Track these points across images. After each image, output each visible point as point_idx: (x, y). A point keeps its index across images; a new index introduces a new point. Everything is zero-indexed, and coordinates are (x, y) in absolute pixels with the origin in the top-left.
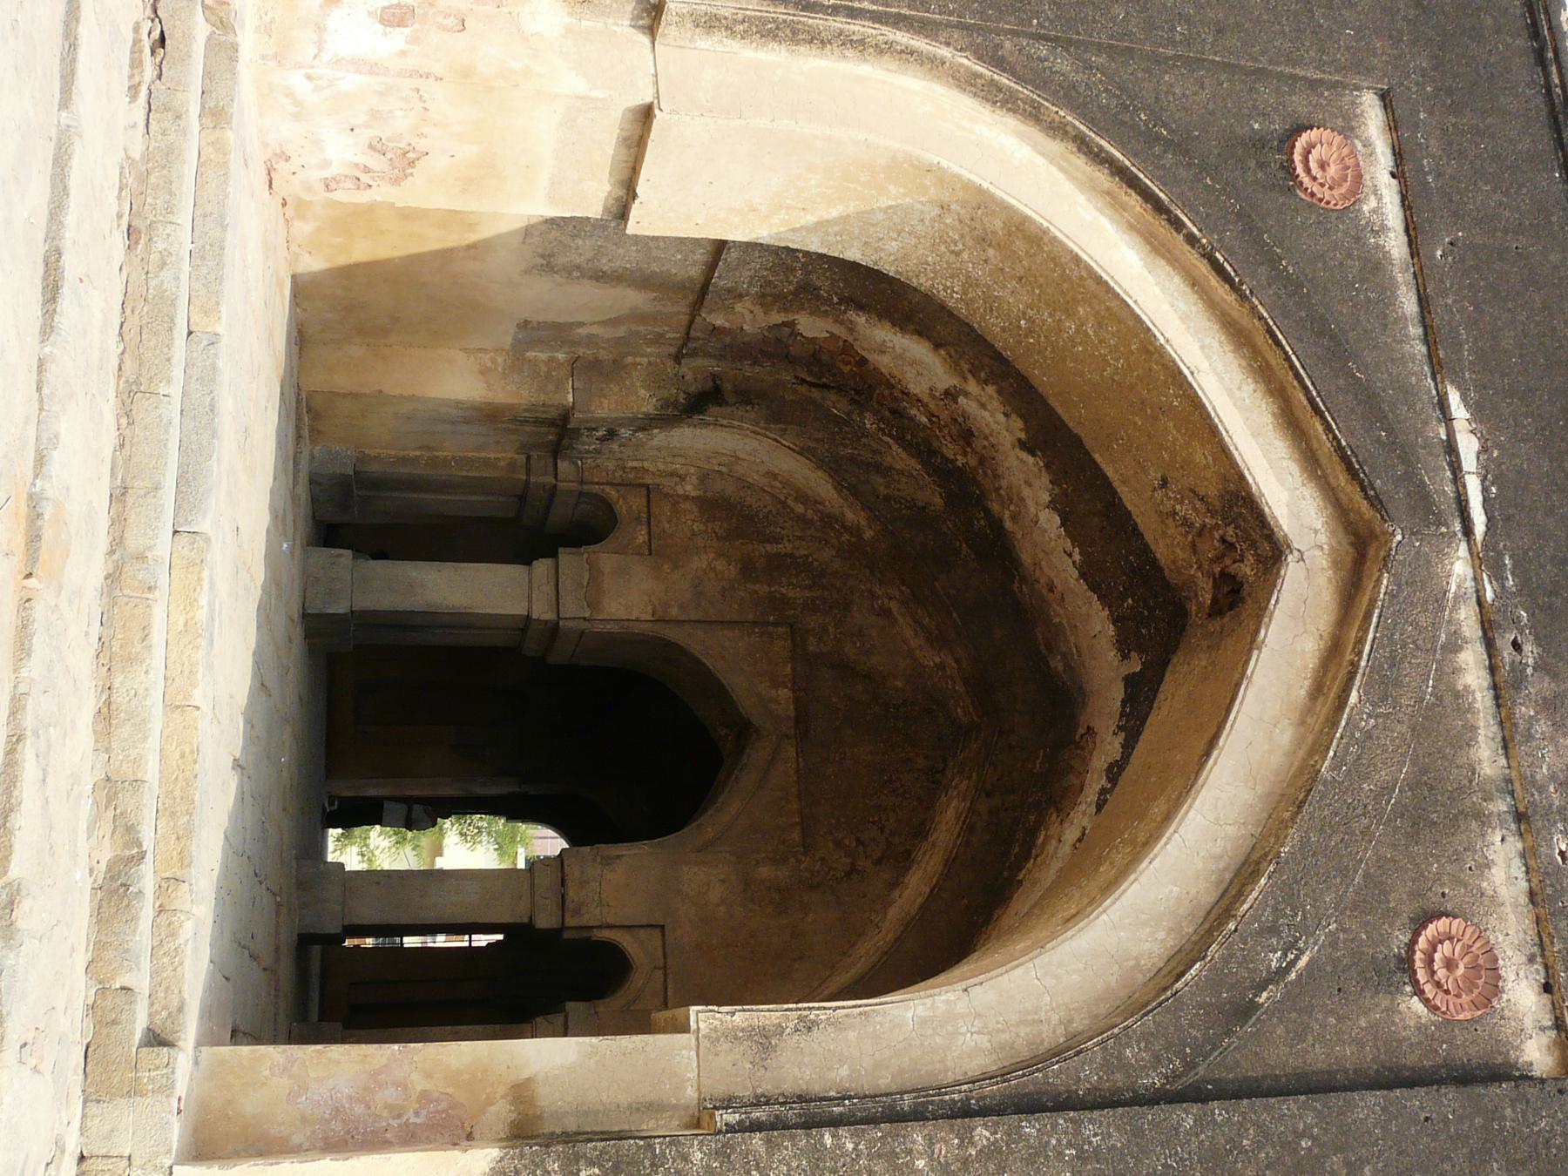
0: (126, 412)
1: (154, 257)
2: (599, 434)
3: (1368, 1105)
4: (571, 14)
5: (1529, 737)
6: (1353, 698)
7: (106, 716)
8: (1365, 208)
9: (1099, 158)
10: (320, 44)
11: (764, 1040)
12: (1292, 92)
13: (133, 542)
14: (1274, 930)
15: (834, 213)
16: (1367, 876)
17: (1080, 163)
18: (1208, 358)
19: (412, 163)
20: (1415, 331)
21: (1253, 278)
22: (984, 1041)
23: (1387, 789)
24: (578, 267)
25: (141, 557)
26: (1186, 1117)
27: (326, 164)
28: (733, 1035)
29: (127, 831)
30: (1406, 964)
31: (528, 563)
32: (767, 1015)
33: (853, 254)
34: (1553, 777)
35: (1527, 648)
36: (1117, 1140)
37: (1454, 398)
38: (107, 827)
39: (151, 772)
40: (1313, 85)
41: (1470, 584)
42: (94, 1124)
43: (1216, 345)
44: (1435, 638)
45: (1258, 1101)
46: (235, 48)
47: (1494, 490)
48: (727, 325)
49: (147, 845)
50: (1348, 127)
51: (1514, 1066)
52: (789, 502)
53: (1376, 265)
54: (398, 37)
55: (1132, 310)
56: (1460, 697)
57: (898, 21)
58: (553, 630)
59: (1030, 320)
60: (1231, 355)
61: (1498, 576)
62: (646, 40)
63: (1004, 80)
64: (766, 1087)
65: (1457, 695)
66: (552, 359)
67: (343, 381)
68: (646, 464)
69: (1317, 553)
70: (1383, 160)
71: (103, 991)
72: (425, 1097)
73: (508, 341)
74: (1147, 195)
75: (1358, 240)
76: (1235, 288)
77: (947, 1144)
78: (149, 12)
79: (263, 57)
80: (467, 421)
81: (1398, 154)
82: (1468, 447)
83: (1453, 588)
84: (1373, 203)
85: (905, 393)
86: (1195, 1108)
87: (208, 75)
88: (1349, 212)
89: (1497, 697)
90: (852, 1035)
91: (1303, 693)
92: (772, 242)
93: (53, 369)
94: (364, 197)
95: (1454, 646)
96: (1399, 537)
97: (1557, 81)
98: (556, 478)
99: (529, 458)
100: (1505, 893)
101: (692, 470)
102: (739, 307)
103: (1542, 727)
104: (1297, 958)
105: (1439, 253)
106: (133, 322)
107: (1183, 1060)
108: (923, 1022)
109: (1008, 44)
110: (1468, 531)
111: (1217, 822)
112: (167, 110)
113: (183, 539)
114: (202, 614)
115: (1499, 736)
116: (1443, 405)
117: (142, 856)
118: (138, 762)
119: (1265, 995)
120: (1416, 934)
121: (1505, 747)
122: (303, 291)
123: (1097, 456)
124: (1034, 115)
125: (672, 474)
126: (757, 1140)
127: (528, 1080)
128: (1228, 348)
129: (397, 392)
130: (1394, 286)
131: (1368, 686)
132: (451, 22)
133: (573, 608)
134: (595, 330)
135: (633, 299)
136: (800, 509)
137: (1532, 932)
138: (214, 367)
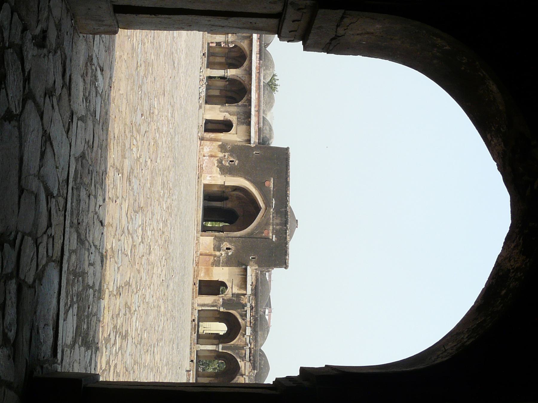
26: (248, 239)
29: (198, 222)
37: (274, 199)
50: (270, 181)
53: (270, 190)
56: (270, 218)
82: (274, 202)
88: (269, 187)
95: (270, 215)
103: (275, 220)
133: (225, 206)
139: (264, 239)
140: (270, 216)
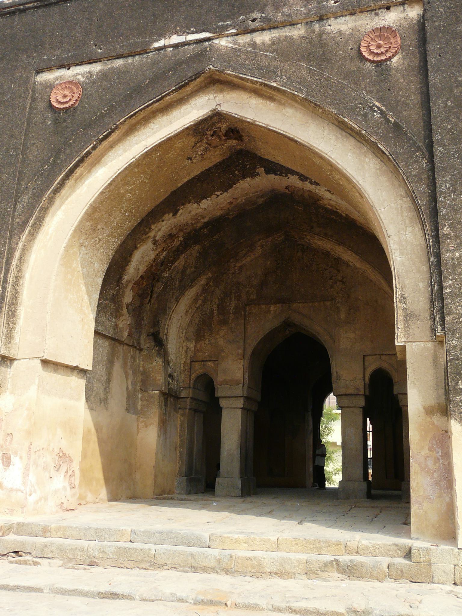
0: (162, 566)
1: (101, 555)
2: (170, 381)
3: (434, 79)
4: (6, 392)
5: (289, 15)
6: (274, 84)
7: (281, 574)
8: (82, 80)
9: (62, 184)
10: (18, 490)
11: (409, 316)
12: (36, 108)
13: (213, 564)
14: (365, 116)
15: (84, 288)
16: (344, 79)
17: (64, 192)
18: (140, 141)
19: (64, 454)
20: (130, 60)
21: (109, 124)
22: (409, 229)
23: (310, 71)
24: (105, 389)
25: (219, 561)
26: (439, 150)
27: (64, 488)
28: (407, 328)
29: (326, 566)
30: (379, 64)
31: (221, 409)
32: (399, 315)
33: (100, 281)
34: (305, 6)
35: (255, 16)
36: (448, 177)
37: (156, 45)
38: (325, 574)
39: (303, 557)
40: (33, 100)
41: (229, 39)
42: (441, 579)
43: (135, 138)
44: (251, 52)
45: (433, 122)
46: (19, 524)
47: (192, 29)
48: (128, 330)
49: (332, 558)
50: (50, 86)
51: (419, 21)
52: (197, 306)
53: (104, 76)
54: (15, 460)
55: (122, 171)
56: (275, 43)
57: (8, 263)
58: (247, 399)
59: (126, 211)
60: (140, 133)
61: (226, 28)
62: (16, 362)
63: (31, 222)
64: (427, 315)
65: (273, 44)
66: (141, 399)
67: (150, 482)
68: (182, 362)
69: (217, 98)
70: (63, 73)
71: (389, 576)
72: (431, 449)
73: (134, 416)
74: (77, 166)
75: (94, 83)
76: (113, 131)
77: (449, 244)
78: (5, 557)
79: (22, 513)
80: (166, 432)
81: (61, 67)
82: (175, 39)
83: (231, 45)
84: (80, 77)
85: (154, 260)
86: (435, 146)
87: (29, 534)
88: (83, 86)
89: (274, 28)
90: (407, 281)
91: (272, 104)
92: (95, 313)
93: (146, 595)
94: (77, 473)
95: (254, 45)
96: (211, 66)
97: (32, 4)
98: (187, 398)
99: (180, 408)
100: (351, 25)
101: (185, 344)
102: (121, 326)
103: (286, 10)
104: (376, 106)
105: (99, 51)
106: (127, 564)
107: (416, 151)
108: (402, 253)
109: (18, 220)
110: (208, 39)
111: (323, 138)
112: (43, 551)
113: (212, 544)
114: (241, 537)
115: (289, 27)
116: (159, 49)
117: (336, 560)
118: (299, 562)
119: (391, 119)
120: (367, 60)
121: (294, 25)
122: (114, 497)
123: (179, 185)
124: (45, 210)
125: (186, 352)
126: (448, 319)
127: (424, 409)
128: (137, 133)
129: (154, 460)
130: (112, 69)
131: (270, 79)
132: (9, 439)
133: (239, 391)
134: (130, 382)
135: (117, 367)
136: (200, 302)
137: (366, 14)
138: (144, 532)
139: (431, 46)
140: (265, 47)
